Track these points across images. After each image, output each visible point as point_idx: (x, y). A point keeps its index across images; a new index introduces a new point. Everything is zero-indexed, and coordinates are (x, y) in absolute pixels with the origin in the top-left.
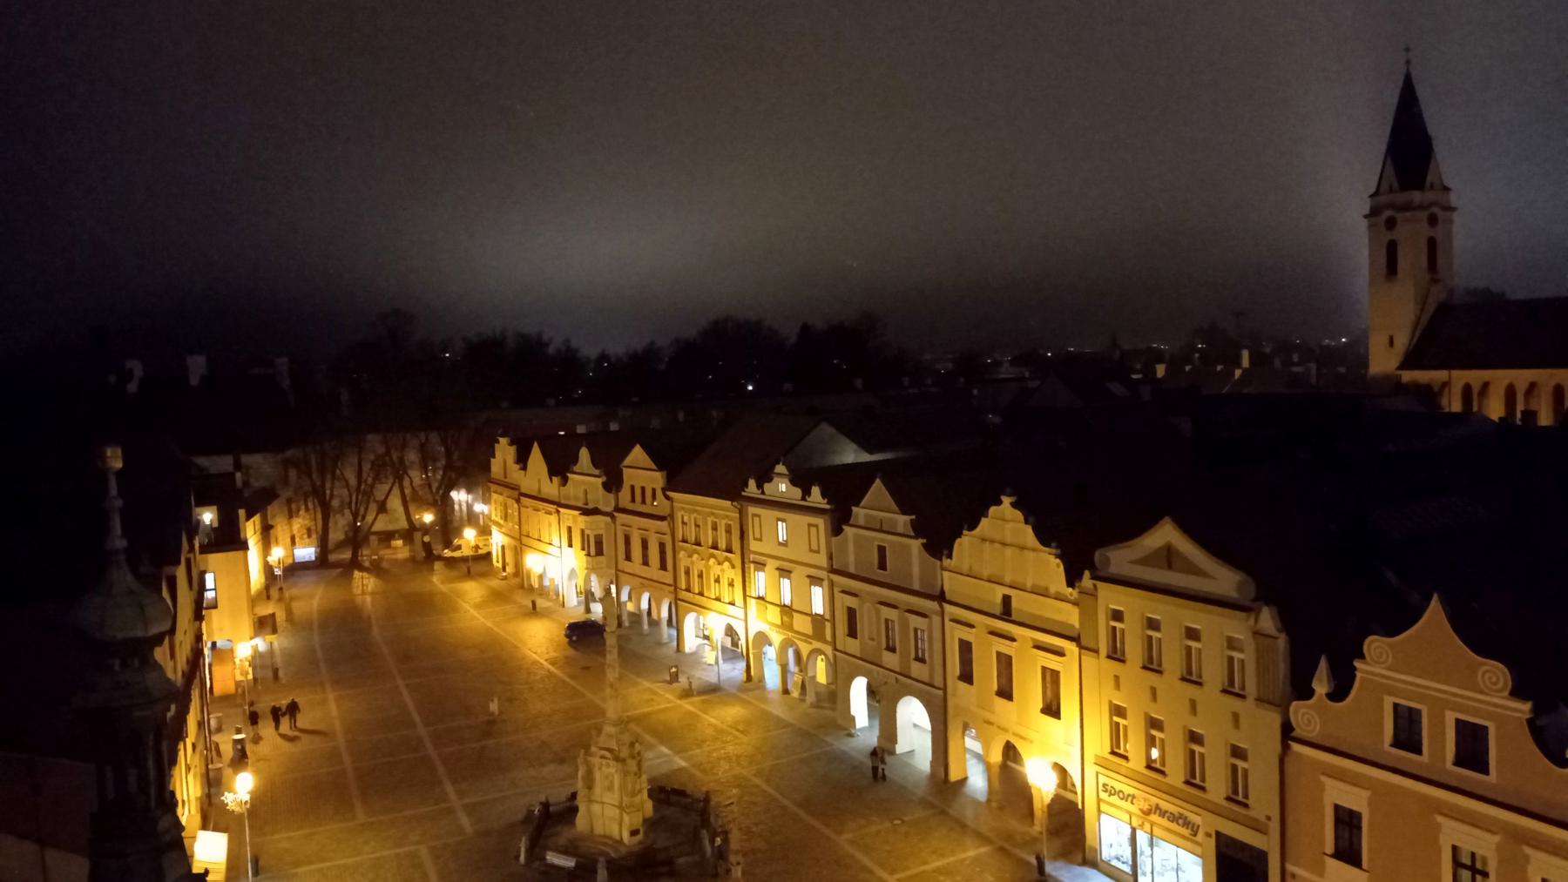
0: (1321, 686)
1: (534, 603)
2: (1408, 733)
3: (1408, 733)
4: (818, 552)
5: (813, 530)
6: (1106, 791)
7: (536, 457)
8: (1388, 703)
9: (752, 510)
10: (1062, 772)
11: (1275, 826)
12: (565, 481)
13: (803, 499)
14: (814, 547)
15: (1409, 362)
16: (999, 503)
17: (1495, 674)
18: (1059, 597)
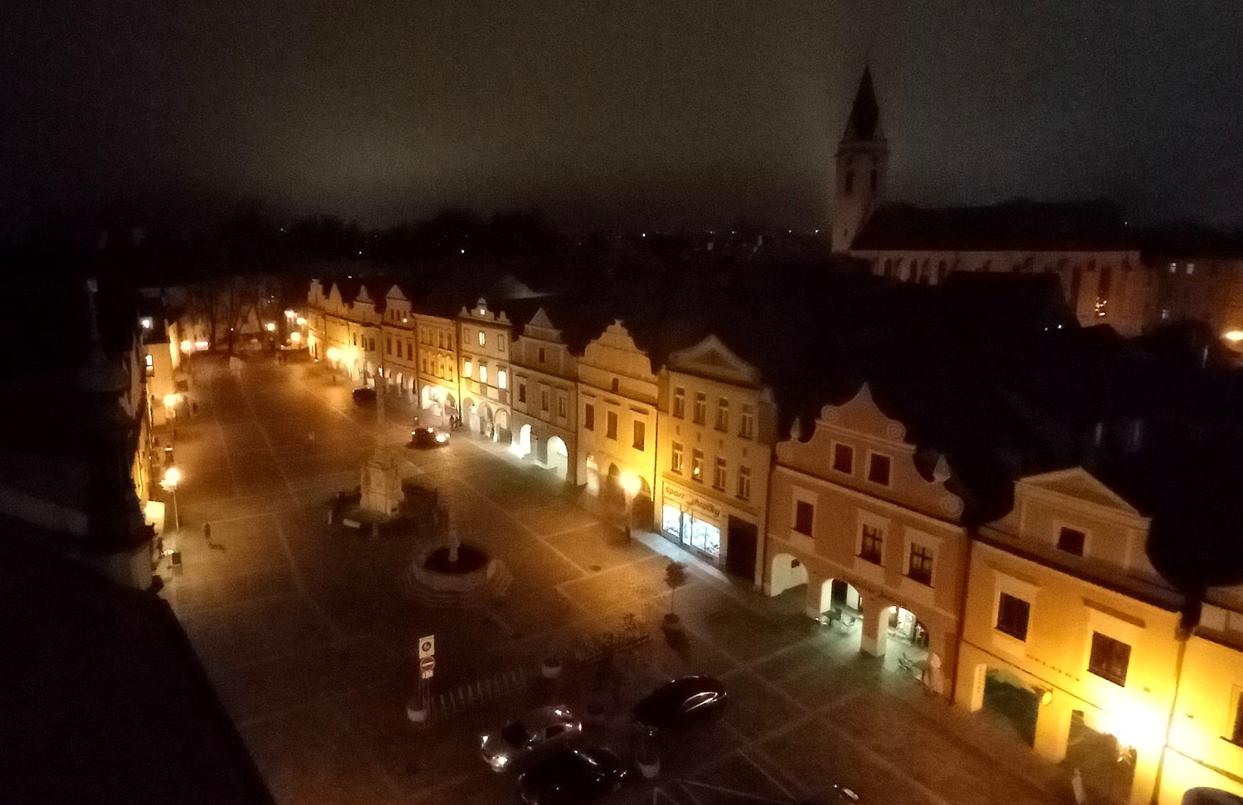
0: (795, 434)
1: (334, 378)
2: (844, 460)
3: (844, 460)
4: (503, 351)
5: (501, 337)
6: (668, 492)
7: (335, 293)
8: (834, 443)
9: (464, 326)
10: (644, 481)
11: (763, 513)
12: (351, 306)
13: (495, 319)
14: (502, 349)
15: (858, 243)
16: (613, 323)
17: (896, 429)
18: (647, 380)
